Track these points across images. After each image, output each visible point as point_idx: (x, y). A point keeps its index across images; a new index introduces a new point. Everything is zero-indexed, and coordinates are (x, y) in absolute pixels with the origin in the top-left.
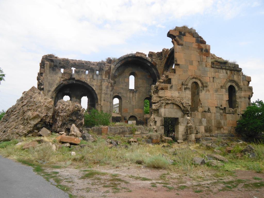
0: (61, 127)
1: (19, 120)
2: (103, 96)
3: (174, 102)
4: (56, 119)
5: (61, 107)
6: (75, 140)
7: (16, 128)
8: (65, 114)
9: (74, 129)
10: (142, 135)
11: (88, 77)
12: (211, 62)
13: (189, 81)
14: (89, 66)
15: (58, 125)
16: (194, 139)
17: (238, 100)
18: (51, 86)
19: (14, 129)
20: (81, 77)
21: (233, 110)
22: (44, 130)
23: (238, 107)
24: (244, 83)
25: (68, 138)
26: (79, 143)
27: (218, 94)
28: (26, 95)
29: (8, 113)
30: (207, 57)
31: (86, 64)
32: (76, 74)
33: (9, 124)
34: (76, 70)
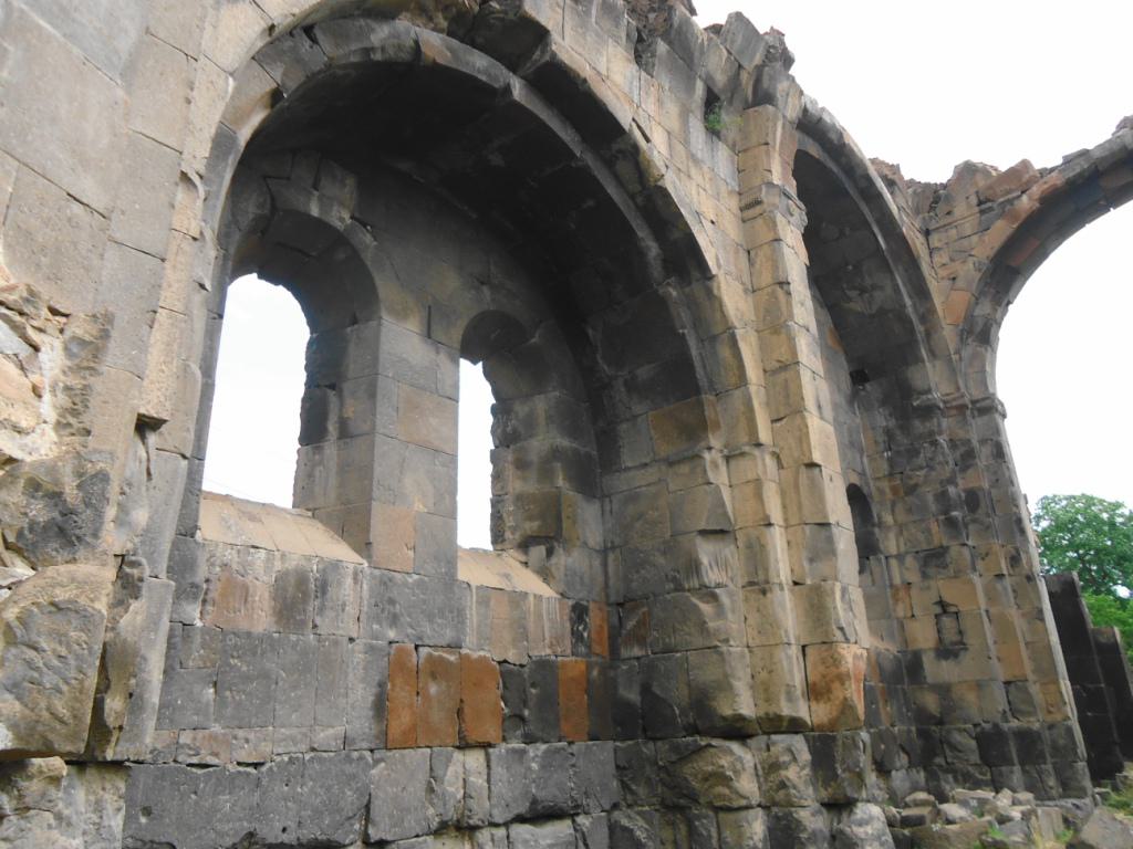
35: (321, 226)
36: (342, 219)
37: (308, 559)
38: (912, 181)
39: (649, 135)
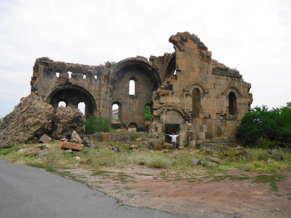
0: (62, 134)
1: (18, 127)
2: (102, 102)
3: (175, 108)
4: (57, 126)
5: (61, 114)
6: (77, 146)
7: (16, 134)
8: (66, 120)
9: (75, 135)
10: (143, 141)
11: (86, 82)
12: (212, 69)
13: (190, 87)
14: (87, 70)
15: (58, 132)
16: (195, 145)
17: (238, 107)
18: (46, 91)
19: (14, 136)
20: (78, 82)
21: (233, 116)
22: (45, 137)
23: (238, 113)
24: (244, 90)
25: (70, 144)
26: (81, 149)
27: (219, 101)
28: (25, 101)
29: (7, 120)
30: (208, 63)
31: (83, 68)
32: (73, 78)
33: (8, 131)
34: (73, 74)
38: (160, 57)
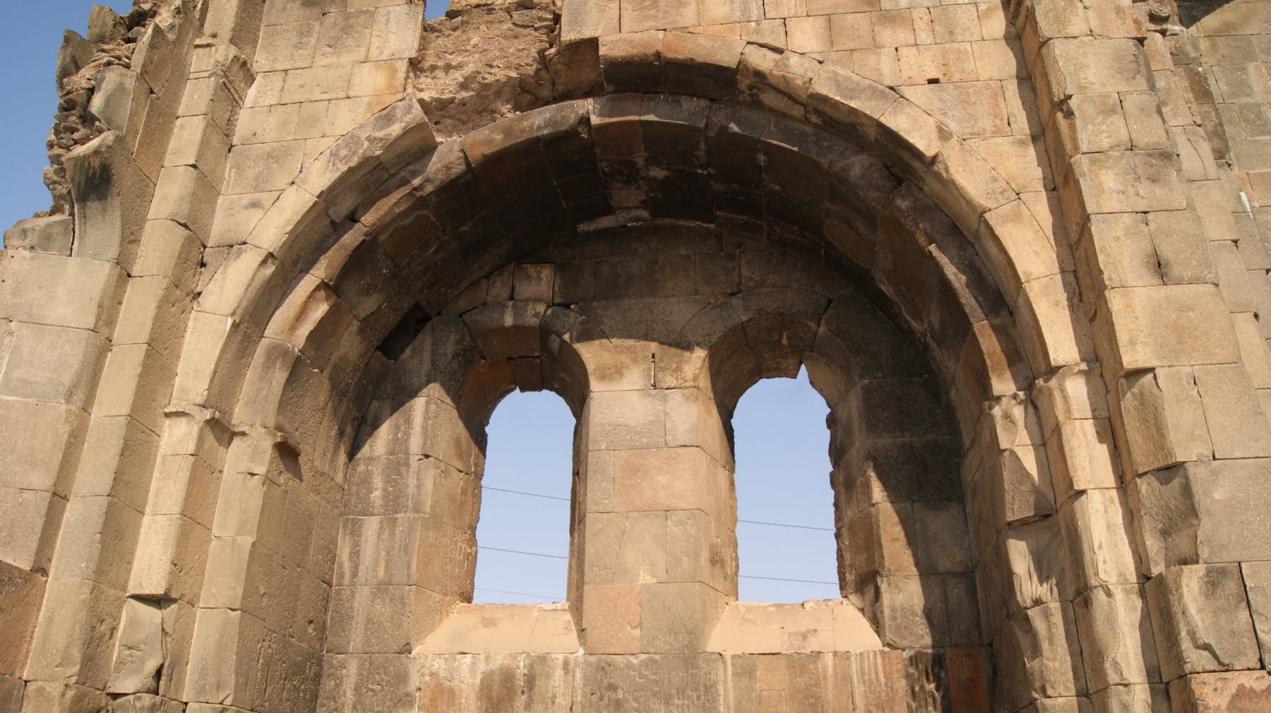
2: (1111, 203)
35: (519, 330)
36: (536, 315)
37: (514, 657)
39: (779, 44)
